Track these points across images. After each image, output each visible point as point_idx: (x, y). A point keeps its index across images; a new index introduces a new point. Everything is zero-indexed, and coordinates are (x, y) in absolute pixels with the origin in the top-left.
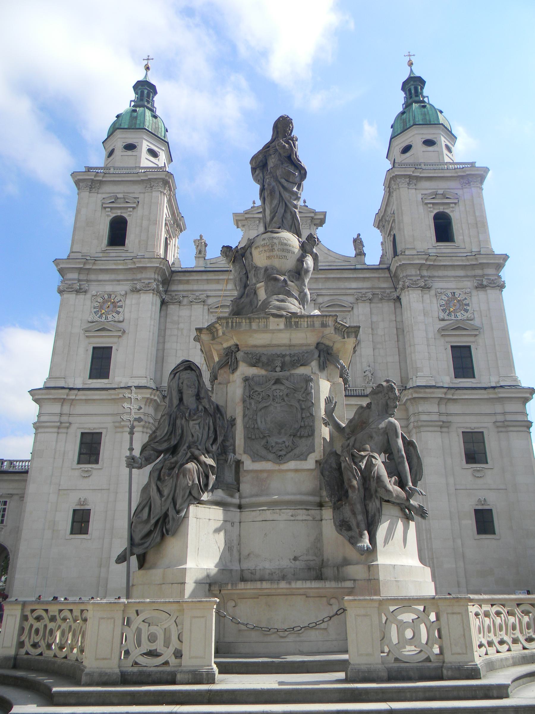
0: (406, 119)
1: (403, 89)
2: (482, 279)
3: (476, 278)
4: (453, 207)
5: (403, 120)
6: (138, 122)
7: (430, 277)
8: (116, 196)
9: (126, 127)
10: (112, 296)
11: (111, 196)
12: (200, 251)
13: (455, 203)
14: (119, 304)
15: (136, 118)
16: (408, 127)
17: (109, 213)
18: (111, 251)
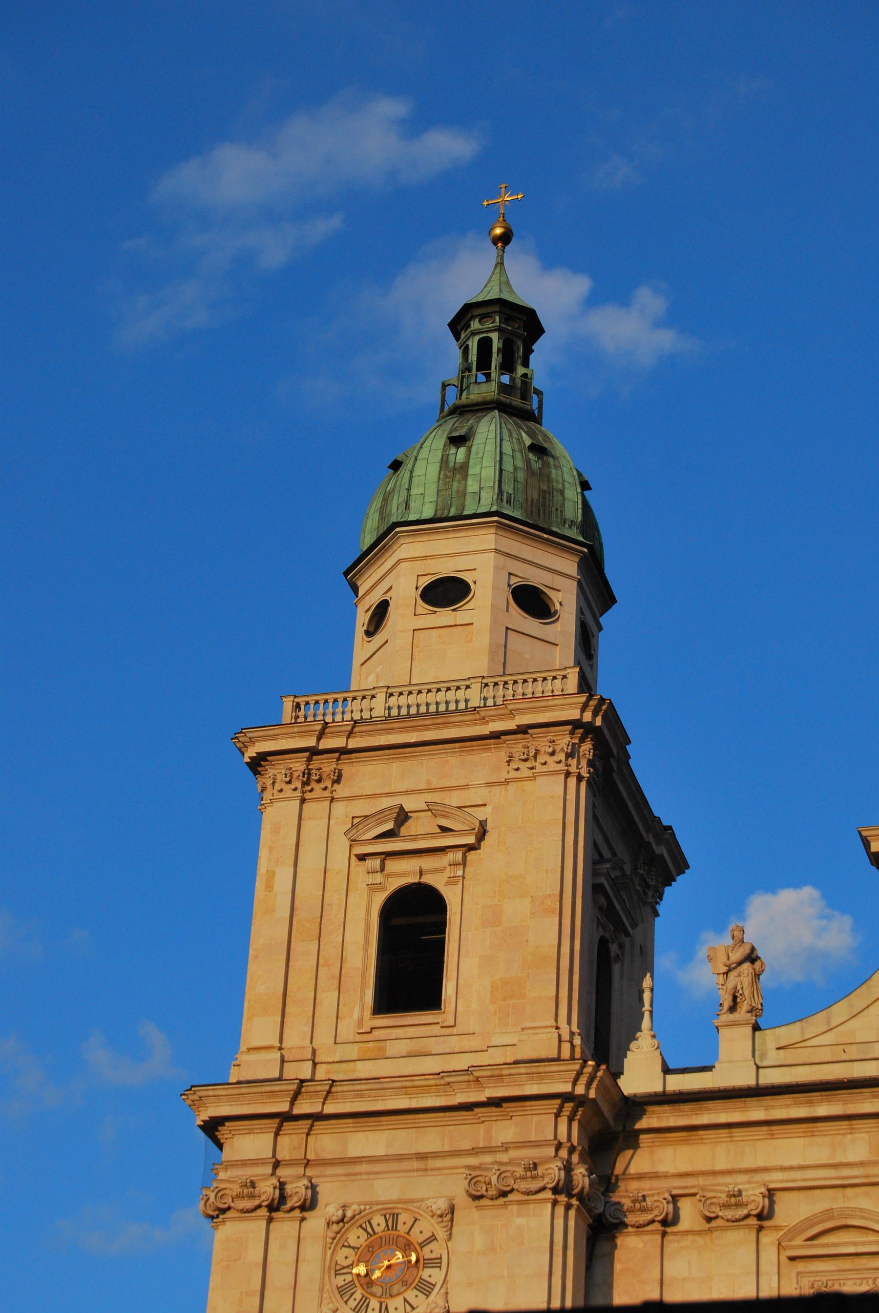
6: (472, 486)
8: (401, 808)
9: (428, 513)
10: (401, 1219)
11: (381, 812)
12: (735, 998)
14: (426, 1253)
17: (378, 878)
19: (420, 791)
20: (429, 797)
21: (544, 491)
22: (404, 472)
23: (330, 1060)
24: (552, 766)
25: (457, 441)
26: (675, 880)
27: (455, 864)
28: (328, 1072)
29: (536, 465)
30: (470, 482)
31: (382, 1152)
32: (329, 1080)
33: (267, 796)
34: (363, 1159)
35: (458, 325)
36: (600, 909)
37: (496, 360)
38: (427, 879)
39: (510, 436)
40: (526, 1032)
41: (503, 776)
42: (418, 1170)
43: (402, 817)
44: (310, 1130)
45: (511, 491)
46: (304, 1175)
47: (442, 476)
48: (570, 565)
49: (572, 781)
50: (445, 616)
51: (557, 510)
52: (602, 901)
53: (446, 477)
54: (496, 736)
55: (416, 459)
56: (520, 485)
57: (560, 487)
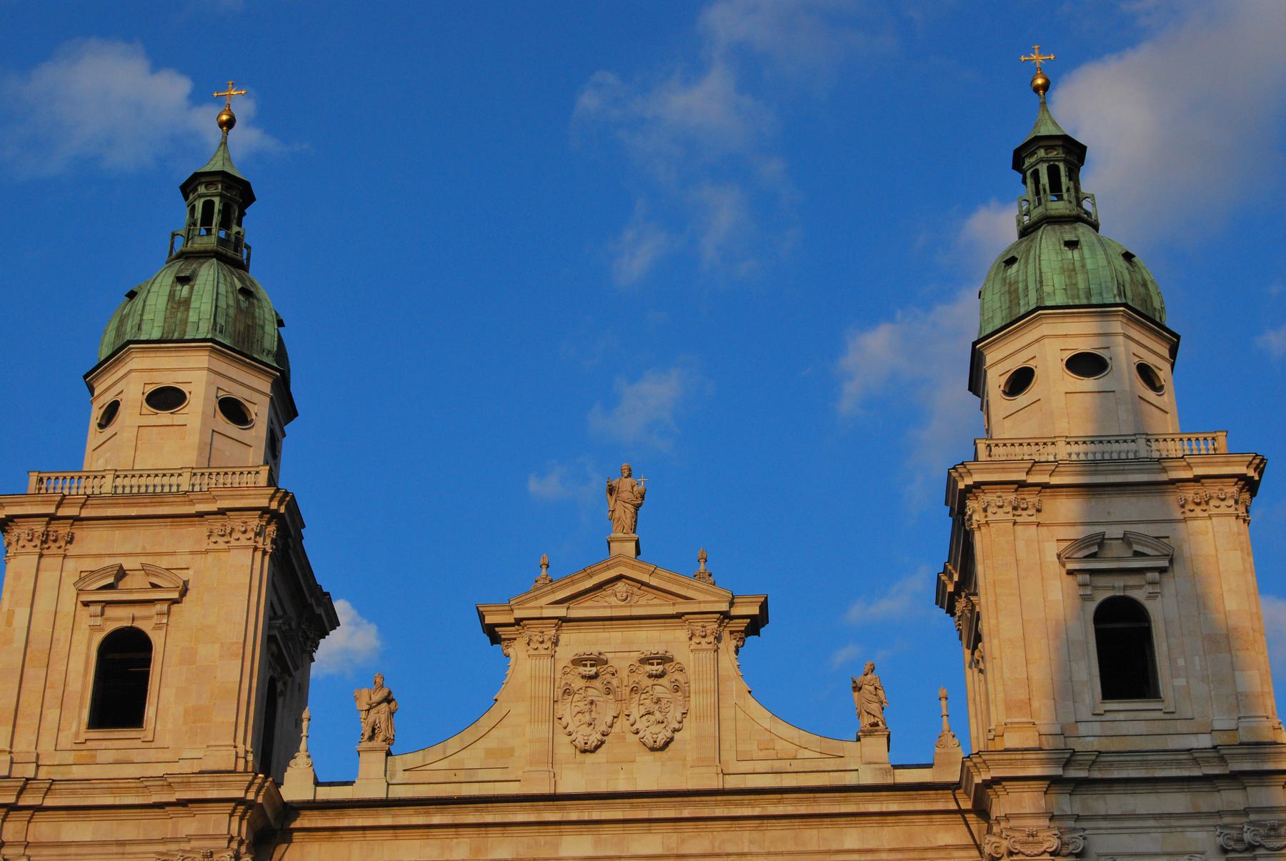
0: (1017, 282)
1: (1018, 164)
2: (1244, 820)
3: (1228, 820)
4: (1153, 583)
5: (1010, 282)
6: (193, 317)
7: (1078, 818)
8: (121, 567)
9: (156, 335)
11: (104, 569)
12: (374, 729)
13: (1162, 570)
15: (186, 303)
16: (1023, 311)
17: (99, 621)
18: (104, 744)
19: (137, 554)
20: (144, 560)
21: (249, 326)
22: (138, 301)
23: (51, 764)
24: (244, 542)
25: (183, 280)
26: (328, 635)
27: (162, 614)
28: (48, 773)
29: (244, 305)
30: (191, 313)
31: (88, 838)
32: (50, 779)
33: (12, 550)
34: (73, 843)
35: (187, 189)
36: (272, 655)
37: (216, 219)
38: (138, 624)
39: (225, 280)
40: (210, 748)
41: (204, 547)
42: (117, 854)
43: (121, 574)
44: (31, 818)
45: (223, 324)
46: (24, 855)
47: (169, 307)
48: (265, 385)
49: (259, 555)
50: (164, 417)
51: (258, 341)
52: (274, 648)
53: (172, 308)
54: (201, 515)
55: (149, 291)
56: (230, 320)
57: (262, 323)
